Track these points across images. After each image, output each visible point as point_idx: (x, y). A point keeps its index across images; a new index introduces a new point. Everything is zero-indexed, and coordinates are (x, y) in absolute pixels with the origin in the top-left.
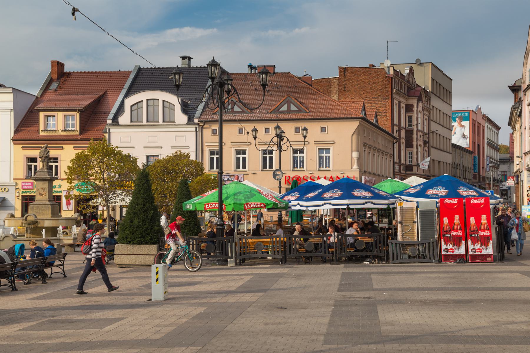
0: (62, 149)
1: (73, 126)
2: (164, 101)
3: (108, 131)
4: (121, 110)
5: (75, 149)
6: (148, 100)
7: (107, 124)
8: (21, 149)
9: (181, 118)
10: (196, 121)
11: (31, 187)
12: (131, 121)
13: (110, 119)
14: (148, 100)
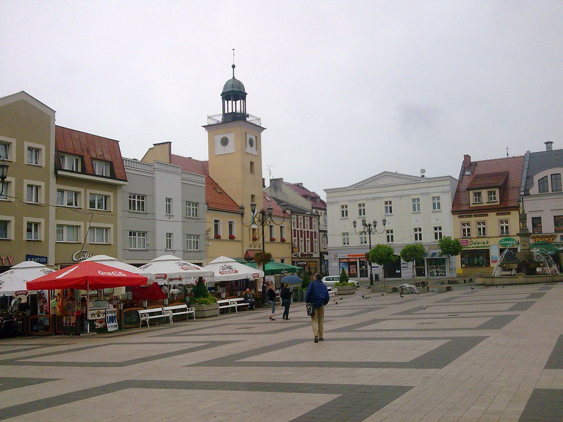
0: (487, 216)
3: (521, 200)
5: (497, 215)
6: (551, 175)
11: (466, 244)
14: (551, 175)
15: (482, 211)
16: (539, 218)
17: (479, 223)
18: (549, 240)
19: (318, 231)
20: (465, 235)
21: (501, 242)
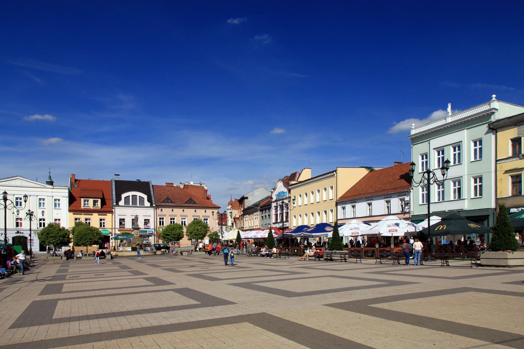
4: (119, 199)
6: (132, 195)
7: (114, 205)
8: (72, 214)
9: (147, 204)
10: (154, 205)
14: (132, 195)
16: (124, 220)
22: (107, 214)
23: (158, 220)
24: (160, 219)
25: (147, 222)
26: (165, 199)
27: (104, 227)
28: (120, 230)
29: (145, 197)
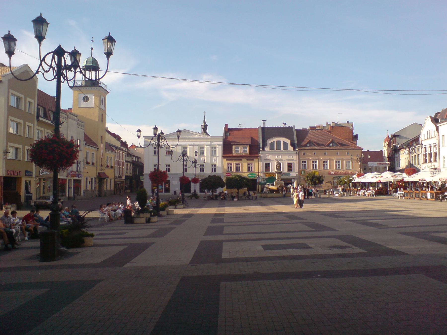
1: (246, 151)
2: (283, 141)
4: (264, 145)
6: (276, 141)
9: (290, 148)
12: (270, 150)
13: (261, 148)
14: (276, 141)
15: (239, 157)
17: (237, 164)
18: (274, 175)
19: (125, 162)
20: (228, 170)
21: (248, 175)
22: (254, 159)
23: (301, 163)
24: (303, 162)
25: (290, 166)
26: (307, 143)
27: (252, 171)
28: (266, 173)
29: (288, 142)
